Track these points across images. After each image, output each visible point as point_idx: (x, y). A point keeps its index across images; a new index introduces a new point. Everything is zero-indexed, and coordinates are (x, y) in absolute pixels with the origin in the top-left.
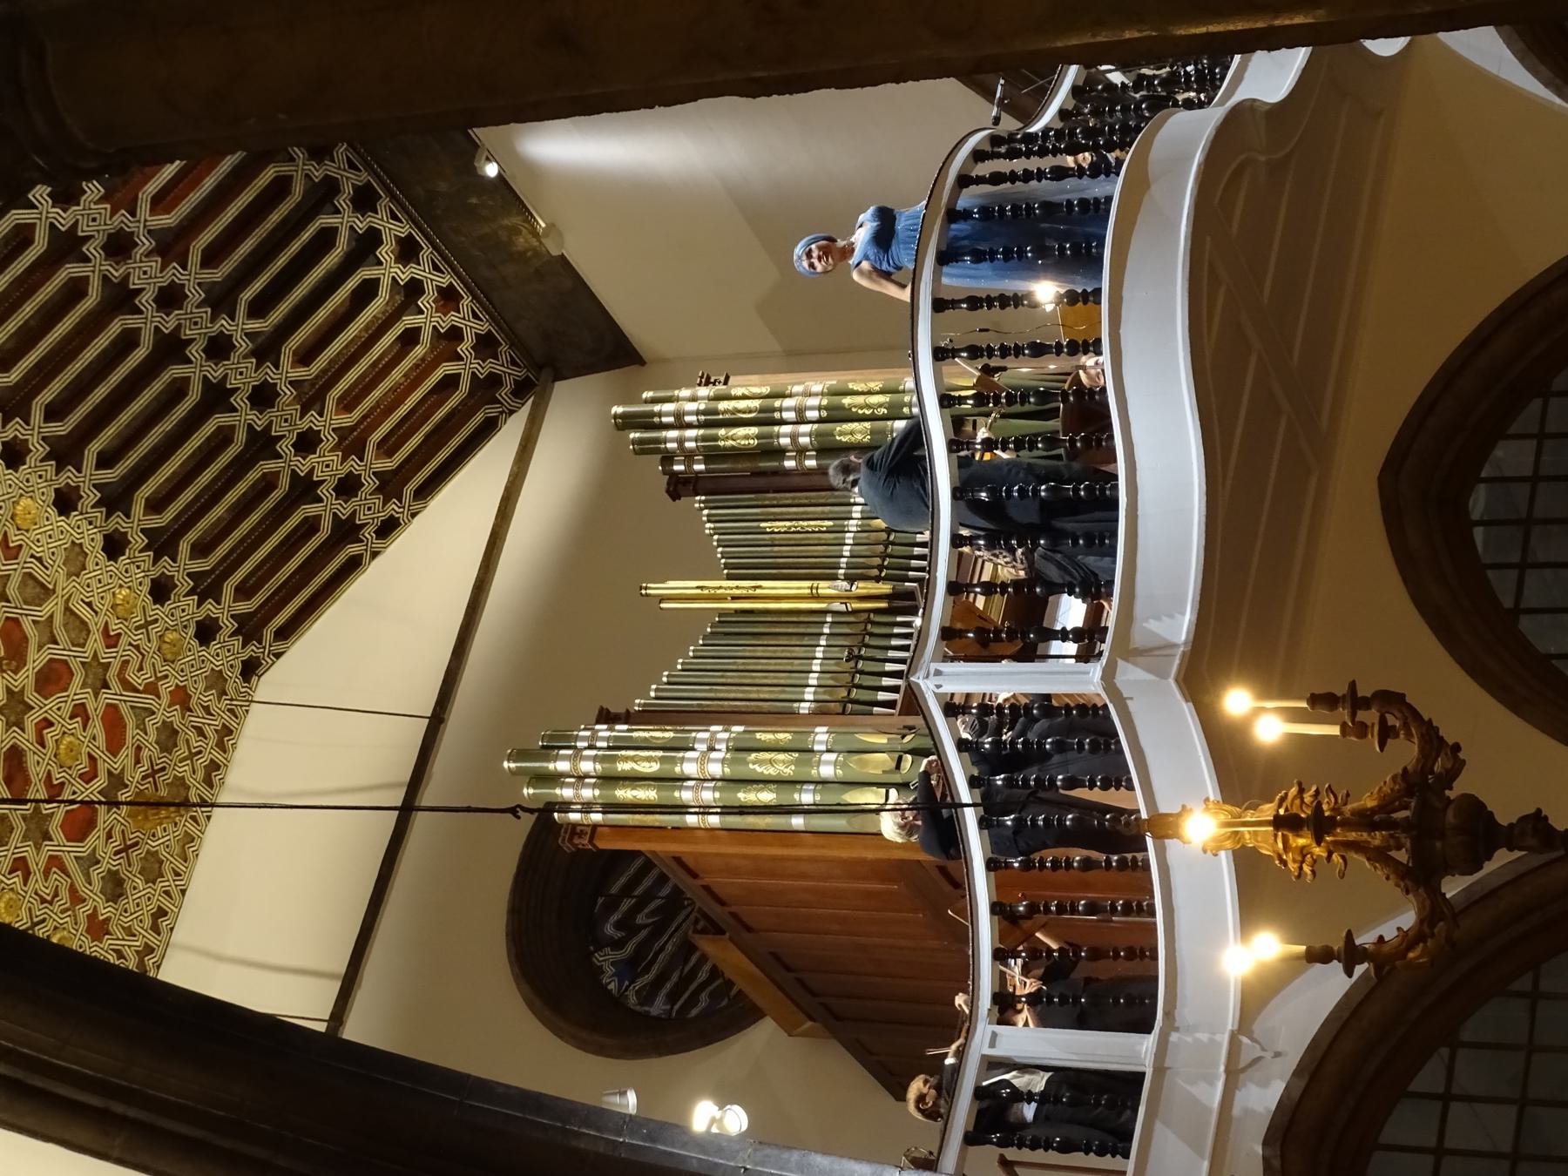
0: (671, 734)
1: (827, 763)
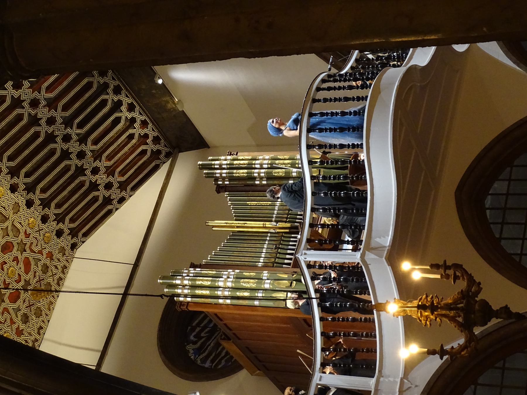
0: (215, 272)
1: (267, 283)
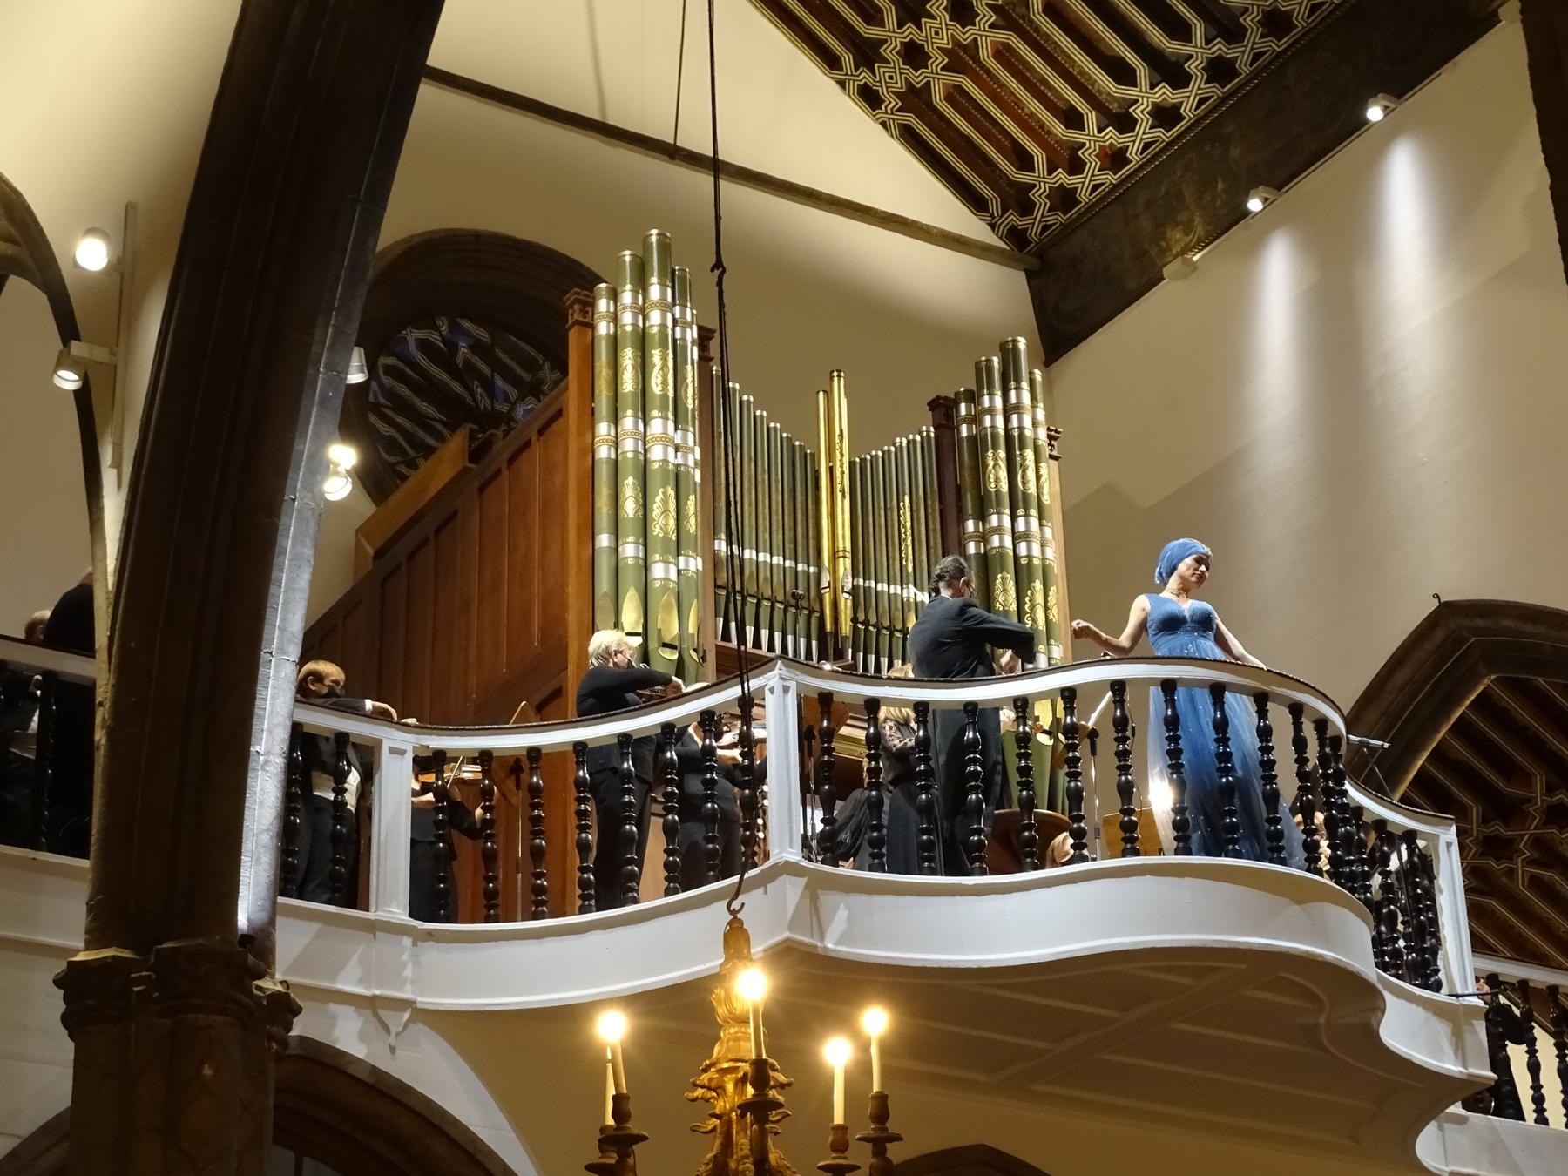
0: (690, 406)
1: (667, 571)
